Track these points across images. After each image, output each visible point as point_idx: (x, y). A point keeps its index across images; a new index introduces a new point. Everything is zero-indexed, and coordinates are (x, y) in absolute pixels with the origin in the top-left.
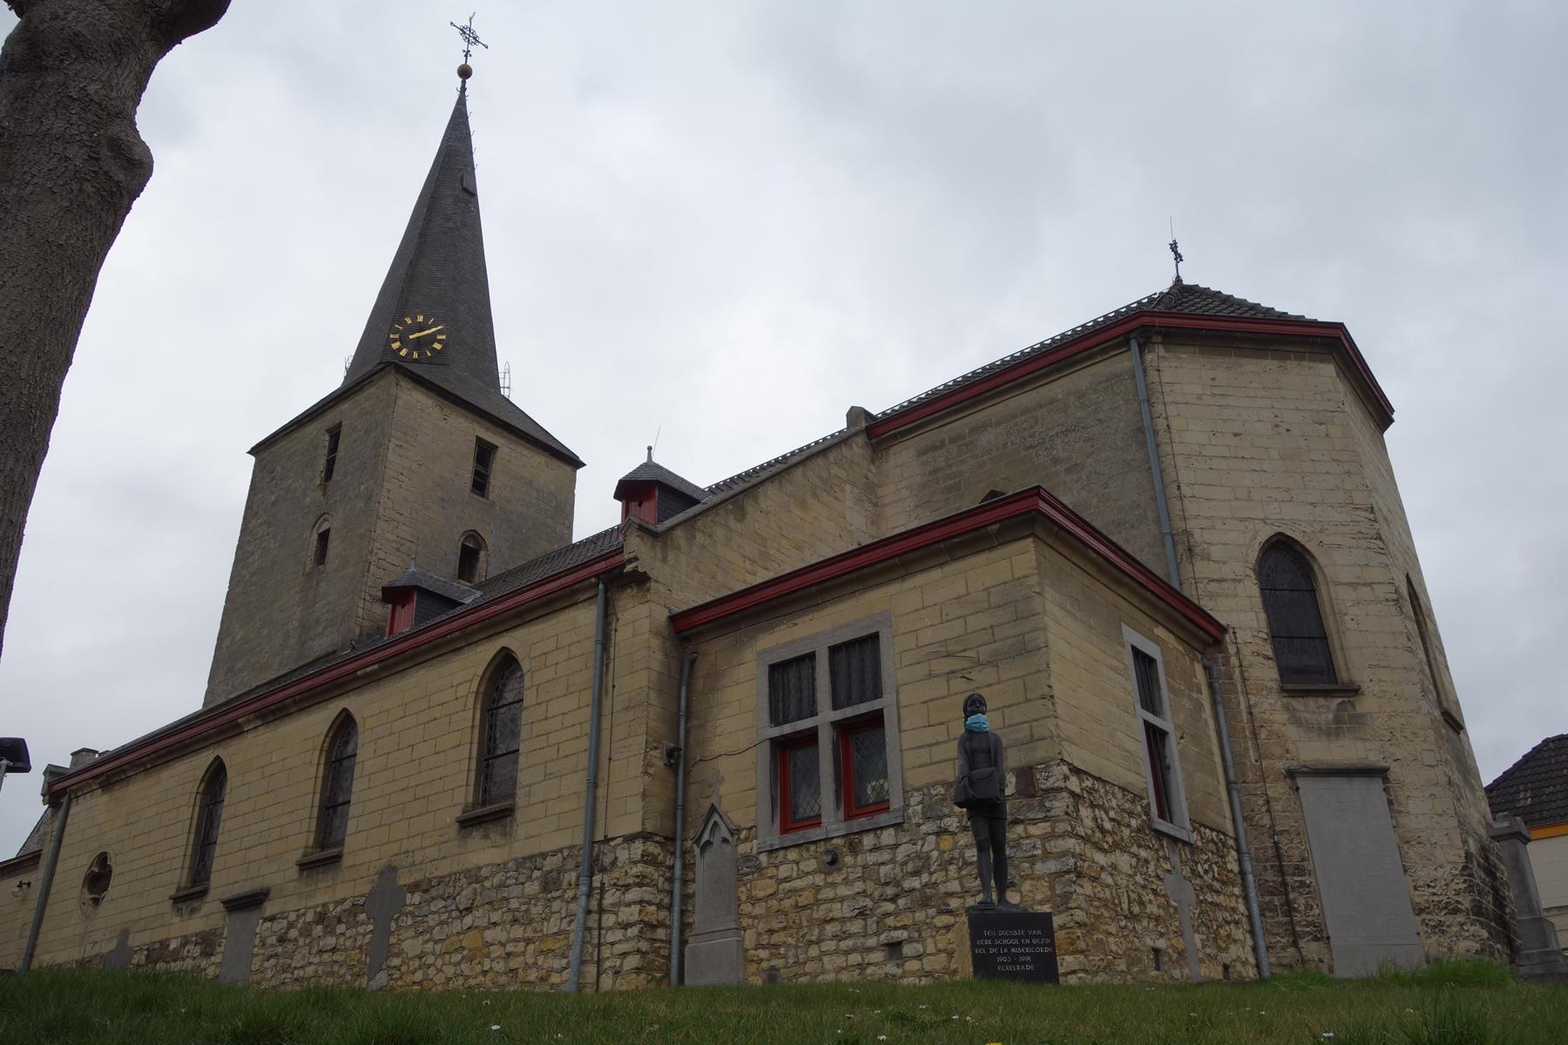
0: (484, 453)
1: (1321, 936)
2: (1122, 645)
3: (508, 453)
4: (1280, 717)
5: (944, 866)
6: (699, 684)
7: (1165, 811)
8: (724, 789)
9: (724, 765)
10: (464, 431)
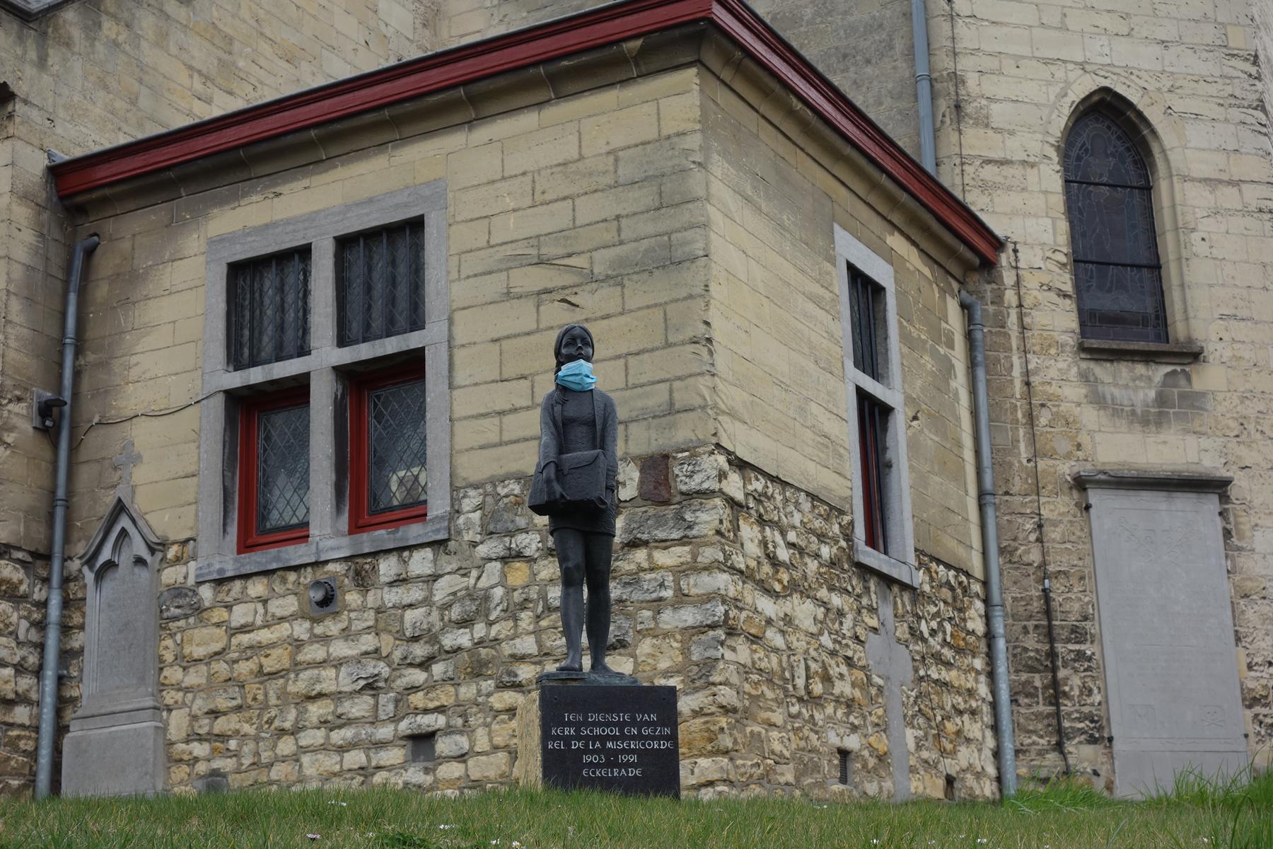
1: (1099, 736)
2: (832, 260)
4: (1074, 392)
5: (512, 613)
6: (101, 291)
7: (877, 534)
8: (140, 475)
9: (143, 434)
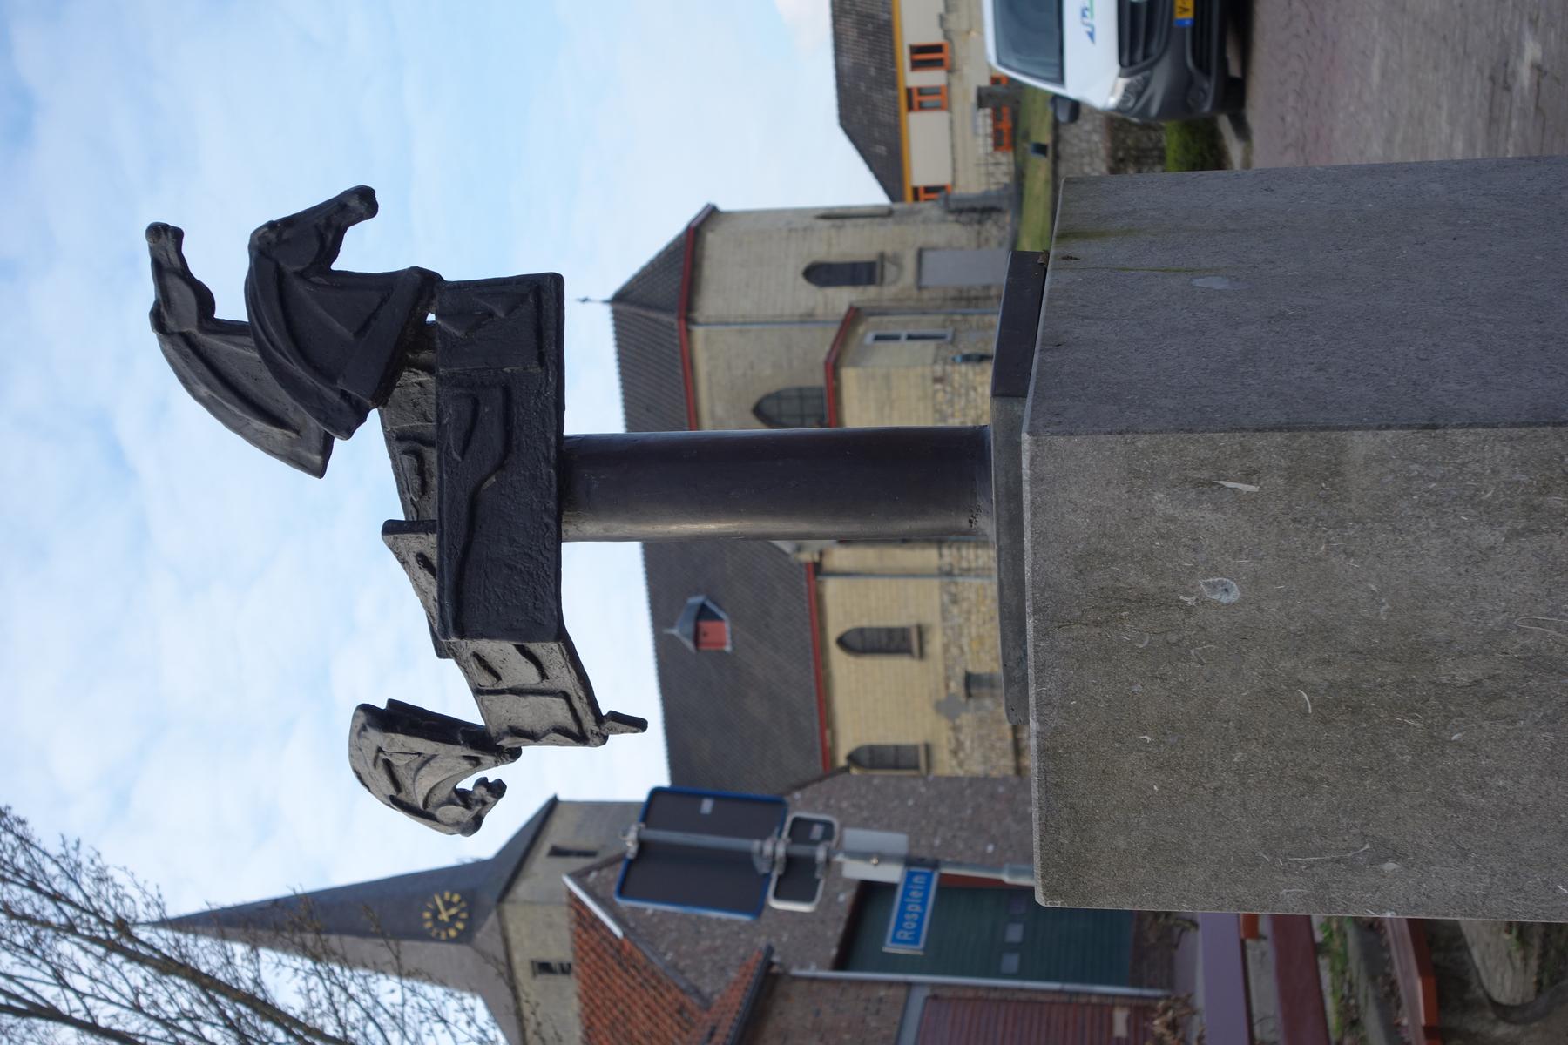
0: (557, 852)
1: (988, 287)
3: (558, 834)
10: (541, 863)
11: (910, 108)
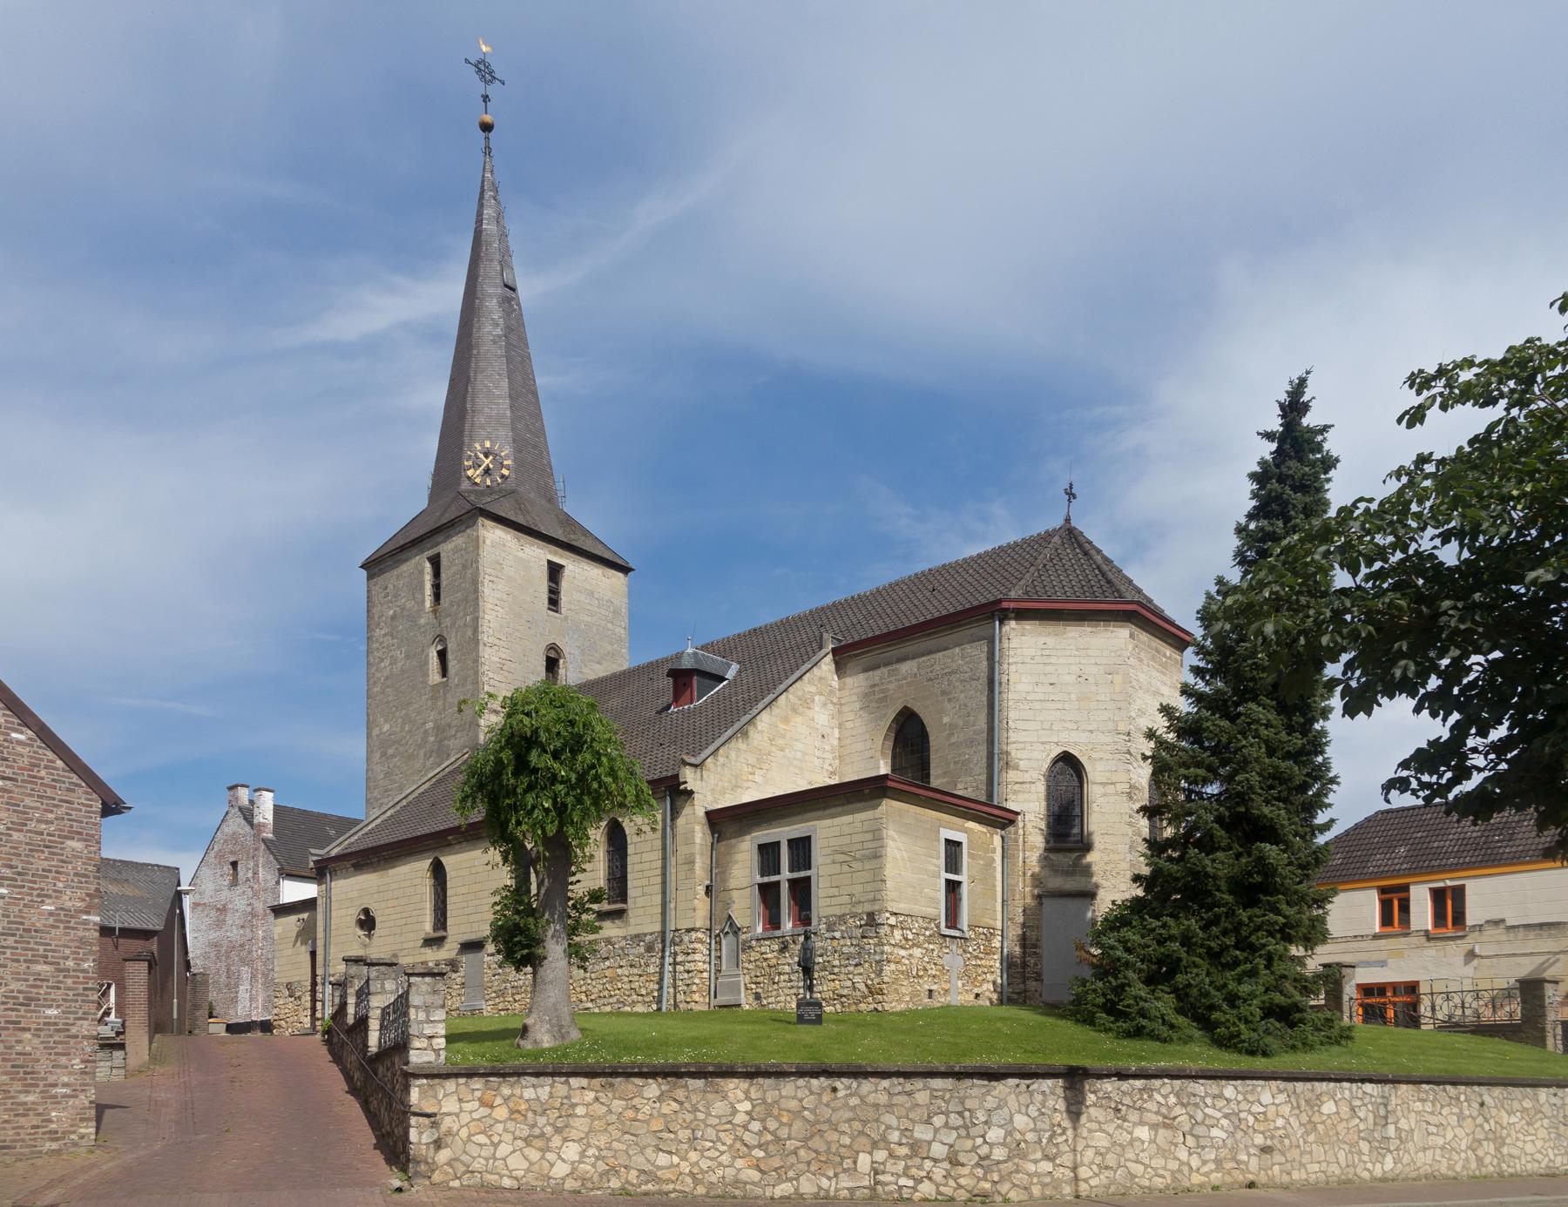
0: (555, 571)
8: (735, 906)
9: (735, 894)
11: (1383, 891)
